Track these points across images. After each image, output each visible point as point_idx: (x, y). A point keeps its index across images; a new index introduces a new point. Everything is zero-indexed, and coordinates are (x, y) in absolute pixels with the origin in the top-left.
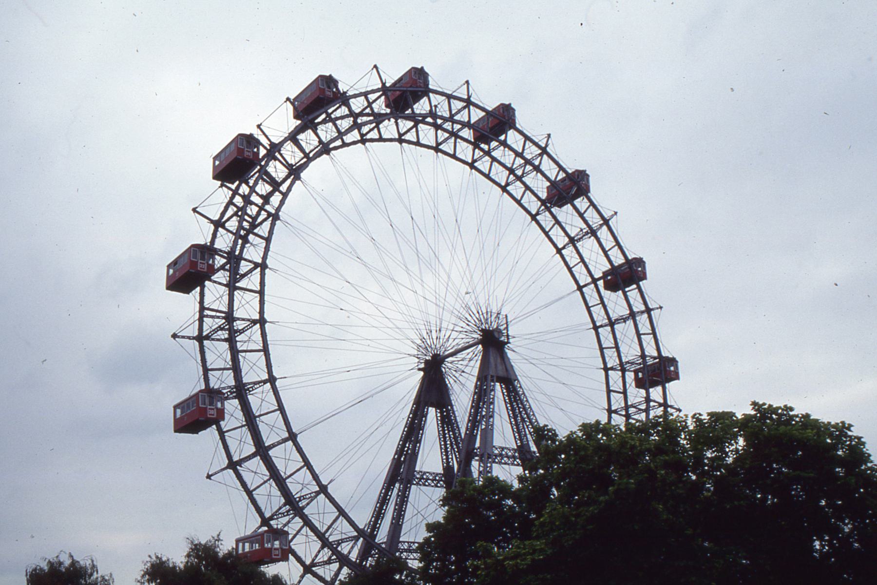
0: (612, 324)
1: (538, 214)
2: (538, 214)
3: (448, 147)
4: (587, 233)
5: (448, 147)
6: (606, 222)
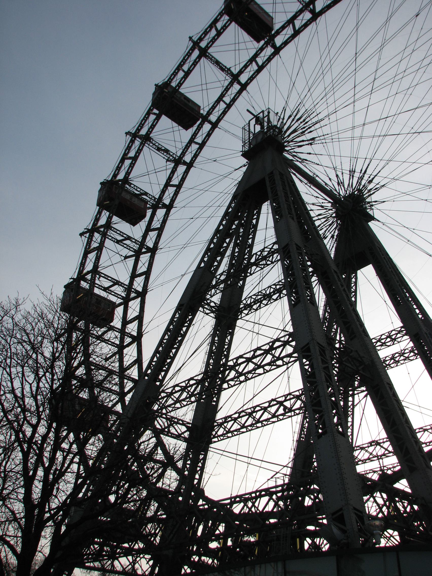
0: (235, 78)
1: (164, 206)
2: (164, 206)
3: (132, 328)
4: (159, 149)
5: (132, 328)
6: (134, 136)
